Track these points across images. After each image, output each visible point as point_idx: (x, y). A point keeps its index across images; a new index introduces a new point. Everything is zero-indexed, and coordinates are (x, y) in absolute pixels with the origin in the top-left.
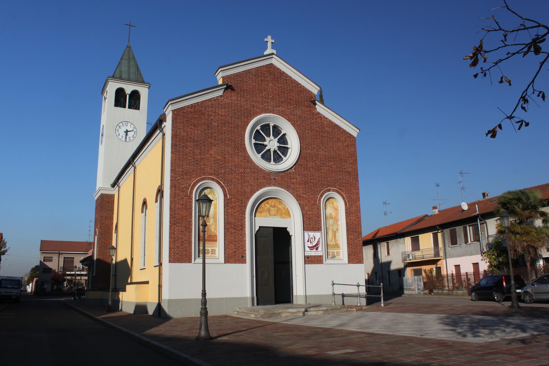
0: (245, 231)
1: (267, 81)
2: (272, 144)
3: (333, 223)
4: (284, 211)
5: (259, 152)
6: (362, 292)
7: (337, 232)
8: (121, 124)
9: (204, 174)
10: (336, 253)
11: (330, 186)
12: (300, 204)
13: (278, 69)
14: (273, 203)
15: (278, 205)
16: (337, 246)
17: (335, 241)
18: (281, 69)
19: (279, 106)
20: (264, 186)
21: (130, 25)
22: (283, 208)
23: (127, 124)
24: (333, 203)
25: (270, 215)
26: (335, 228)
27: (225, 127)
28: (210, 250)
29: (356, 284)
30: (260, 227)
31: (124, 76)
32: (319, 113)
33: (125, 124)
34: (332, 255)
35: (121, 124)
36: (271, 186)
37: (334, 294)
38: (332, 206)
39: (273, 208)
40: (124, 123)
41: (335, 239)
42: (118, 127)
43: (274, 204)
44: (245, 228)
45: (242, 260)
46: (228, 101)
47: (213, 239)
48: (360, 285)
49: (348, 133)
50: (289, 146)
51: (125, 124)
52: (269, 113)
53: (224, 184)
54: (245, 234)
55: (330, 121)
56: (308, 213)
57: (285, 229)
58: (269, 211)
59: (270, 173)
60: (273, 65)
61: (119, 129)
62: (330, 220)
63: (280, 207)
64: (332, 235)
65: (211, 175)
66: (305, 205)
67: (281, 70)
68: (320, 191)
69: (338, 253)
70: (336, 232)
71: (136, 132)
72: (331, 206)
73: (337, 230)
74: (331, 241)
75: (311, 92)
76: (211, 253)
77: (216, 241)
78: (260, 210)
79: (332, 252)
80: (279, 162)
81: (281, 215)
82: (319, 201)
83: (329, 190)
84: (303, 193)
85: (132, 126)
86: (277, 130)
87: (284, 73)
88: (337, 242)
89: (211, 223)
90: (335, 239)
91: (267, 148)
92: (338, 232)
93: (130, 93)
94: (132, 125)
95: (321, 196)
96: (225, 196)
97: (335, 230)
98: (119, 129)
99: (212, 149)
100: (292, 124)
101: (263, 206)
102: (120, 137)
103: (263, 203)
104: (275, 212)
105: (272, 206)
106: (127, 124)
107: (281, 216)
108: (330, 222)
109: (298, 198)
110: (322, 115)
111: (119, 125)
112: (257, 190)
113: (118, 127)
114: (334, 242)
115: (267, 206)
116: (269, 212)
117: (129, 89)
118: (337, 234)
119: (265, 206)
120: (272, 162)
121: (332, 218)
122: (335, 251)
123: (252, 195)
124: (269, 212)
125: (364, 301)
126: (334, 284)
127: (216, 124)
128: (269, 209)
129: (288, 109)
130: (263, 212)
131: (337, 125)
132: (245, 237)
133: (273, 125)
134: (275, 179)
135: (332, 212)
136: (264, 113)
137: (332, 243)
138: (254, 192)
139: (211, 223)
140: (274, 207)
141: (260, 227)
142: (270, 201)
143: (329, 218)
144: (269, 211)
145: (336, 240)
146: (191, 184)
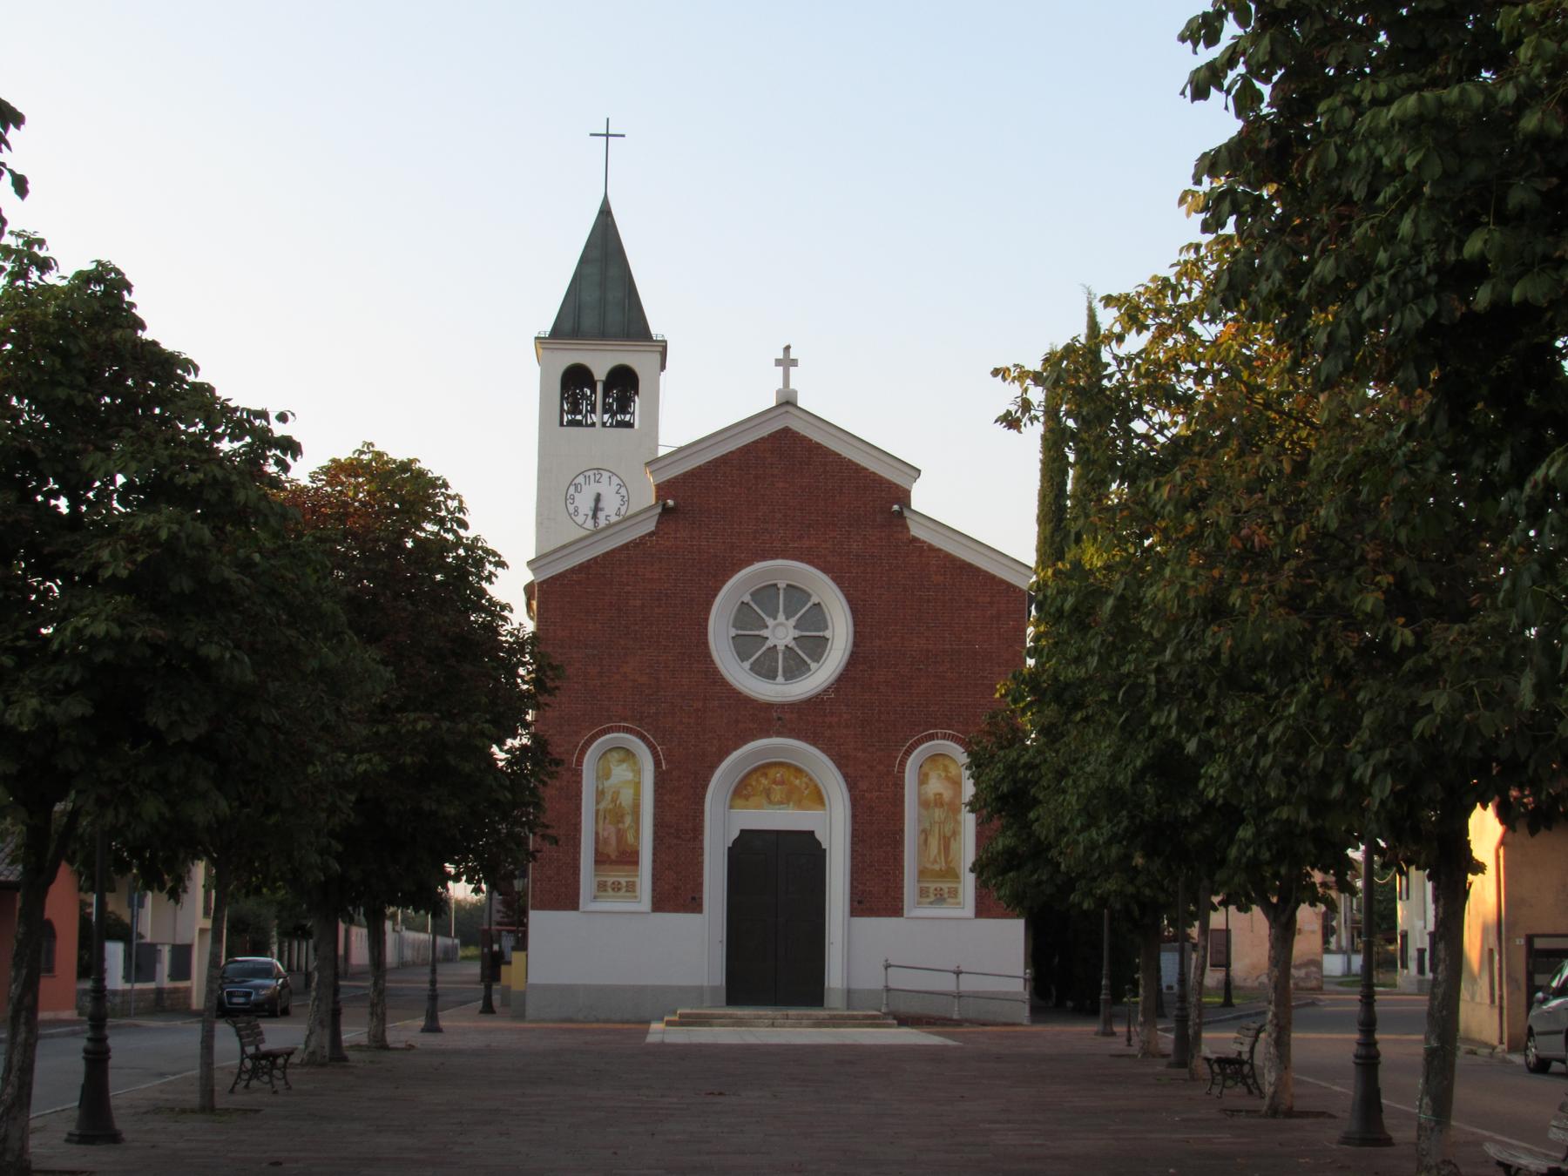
0: (702, 841)
1: (773, 475)
2: (781, 633)
3: (943, 817)
4: (806, 792)
5: (743, 656)
6: (967, 989)
7: (952, 839)
8: (581, 477)
9: (610, 719)
10: (946, 890)
11: (935, 727)
12: (846, 776)
13: (804, 439)
14: (778, 775)
15: (792, 778)
16: (951, 873)
17: (946, 862)
18: (811, 437)
19: (801, 537)
20: (754, 738)
21: (607, 135)
22: (804, 785)
23: (598, 477)
24: (946, 769)
25: (770, 802)
26: (948, 829)
27: (659, 606)
28: (624, 884)
29: (953, 968)
30: (742, 831)
31: (589, 321)
32: (915, 540)
33: (592, 477)
34: (936, 895)
35: (580, 479)
36: (770, 736)
37: (888, 990)
38: (943, 774)
39: (779, 787)
40: (591, 473)
41: (947, 856)
42: (572, 488)
43: (782, 776)
44: (702, 833)
45: (693, 903)
46: (667, 543)
47: (630, 858)
48: (964, 970)
49: (1002, 582)
50: (828, 634)
51: (592, 477)
52: (772, 558)
53: (654, 738)
54: (702, 848)
55: (948, 556)
56: (866, 794)
57: (812, 833)
58: (768, 793)
59: (769, 706)
60: (790, 429)
61: (576, 495)
62: (937, 810)
63: (797, 782)
64: (939, 844)
65: (625, 720)
66: (861, 777)
67: (811, 440)
68: (905, 740)
69: (954, 893)
70: (949, 839)
71: (626, 499)
72: (940, 776)
73: (955, 833)
74: (935, 861)
75: (895, 484)
76: (624, 890)
77: (636, 863)
78: (745, 792)
79: (941, 889)
80: (804, 673)
81: (800, 801)
82: (899, 764)
83: (931, 737)
84: (855, 749)
85: (615, 480)
86: (796, 594)
87: (819, 446)
88: (952, 865)
89: (627, 825)
90: (947, 856)
91: (769, 644)
92: (955, 840)
93: (604, 378)
94: (614, 478)
95: (908, 753)
96: (657, 764)
97: (948, 834)
98: (576, 495)
99: (627, 663)
100: (834, 579)
101: (754, 783)
102: (580, 519)
103: (755, 777)
104: (784, 796)
105: (775, 782)
106: (598, 477)
107: (799, 805)
108: (937, 815)
109: (841, 762)
110: (925, 542)
111: (577, 481)
112: (735, 749)
113: (572, 488)
114: (944, 864)
115: (764, 781)
116: (768, 797)
117: (600, 362)
118: (953, 845)
119: (757, 780)
120: (780, 679)
121: (942, 805)
122: (945, 886)
123: (720, 760)
124: (768, 797)
125: (1025, 1011)
126: (887, 966)
127: (638, 603)
128: (769, 789)
129: (825, 541)
130: (753, 795)
131: (970, 566)
132: (702, 855)
133: (784, 586)
134: (779, 719)
135: (942, 791)
136: (758, 561)
137: (937, 867)
138: (728, 753)
139: (627, 825)
140: (782, 783)
141: (742, 831)
142: (772, 772)
143: (932, 805)
144: (768, 793)
145: (950, 859)
146: (578, 743)
